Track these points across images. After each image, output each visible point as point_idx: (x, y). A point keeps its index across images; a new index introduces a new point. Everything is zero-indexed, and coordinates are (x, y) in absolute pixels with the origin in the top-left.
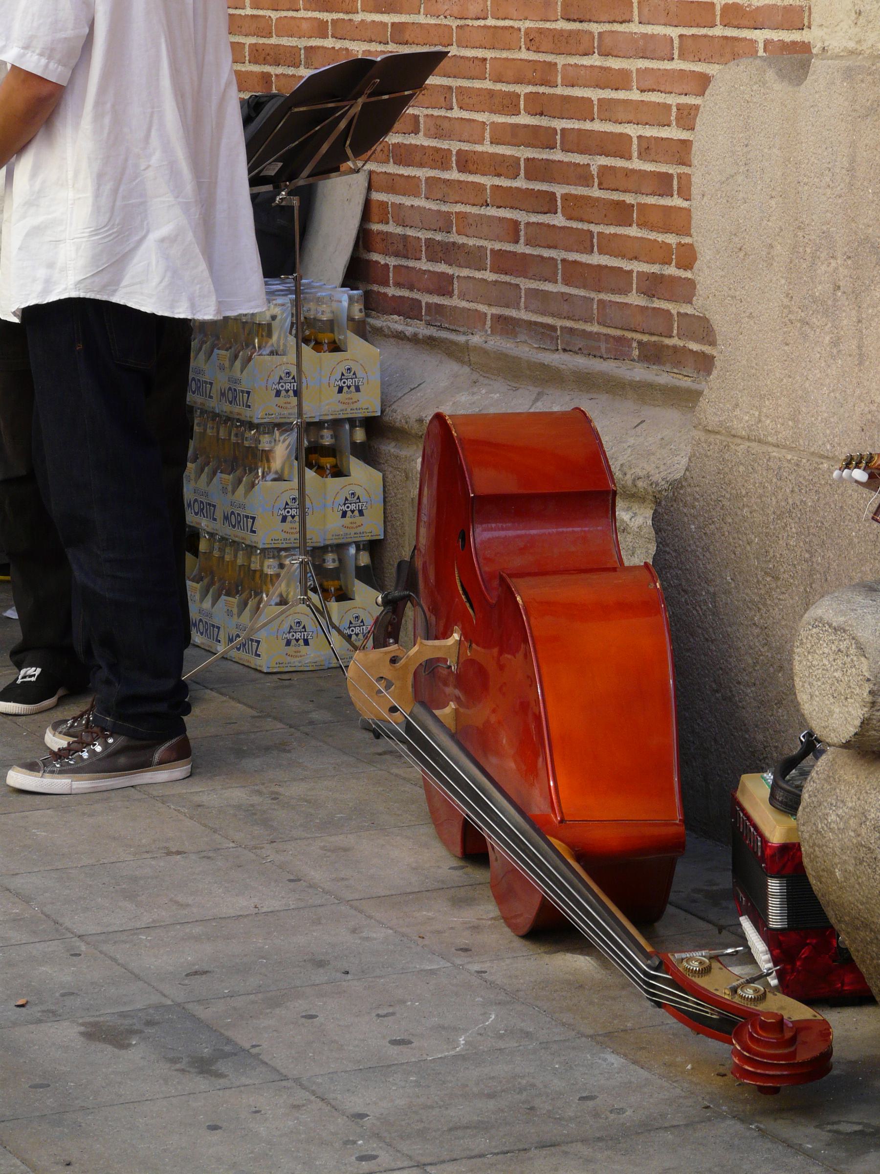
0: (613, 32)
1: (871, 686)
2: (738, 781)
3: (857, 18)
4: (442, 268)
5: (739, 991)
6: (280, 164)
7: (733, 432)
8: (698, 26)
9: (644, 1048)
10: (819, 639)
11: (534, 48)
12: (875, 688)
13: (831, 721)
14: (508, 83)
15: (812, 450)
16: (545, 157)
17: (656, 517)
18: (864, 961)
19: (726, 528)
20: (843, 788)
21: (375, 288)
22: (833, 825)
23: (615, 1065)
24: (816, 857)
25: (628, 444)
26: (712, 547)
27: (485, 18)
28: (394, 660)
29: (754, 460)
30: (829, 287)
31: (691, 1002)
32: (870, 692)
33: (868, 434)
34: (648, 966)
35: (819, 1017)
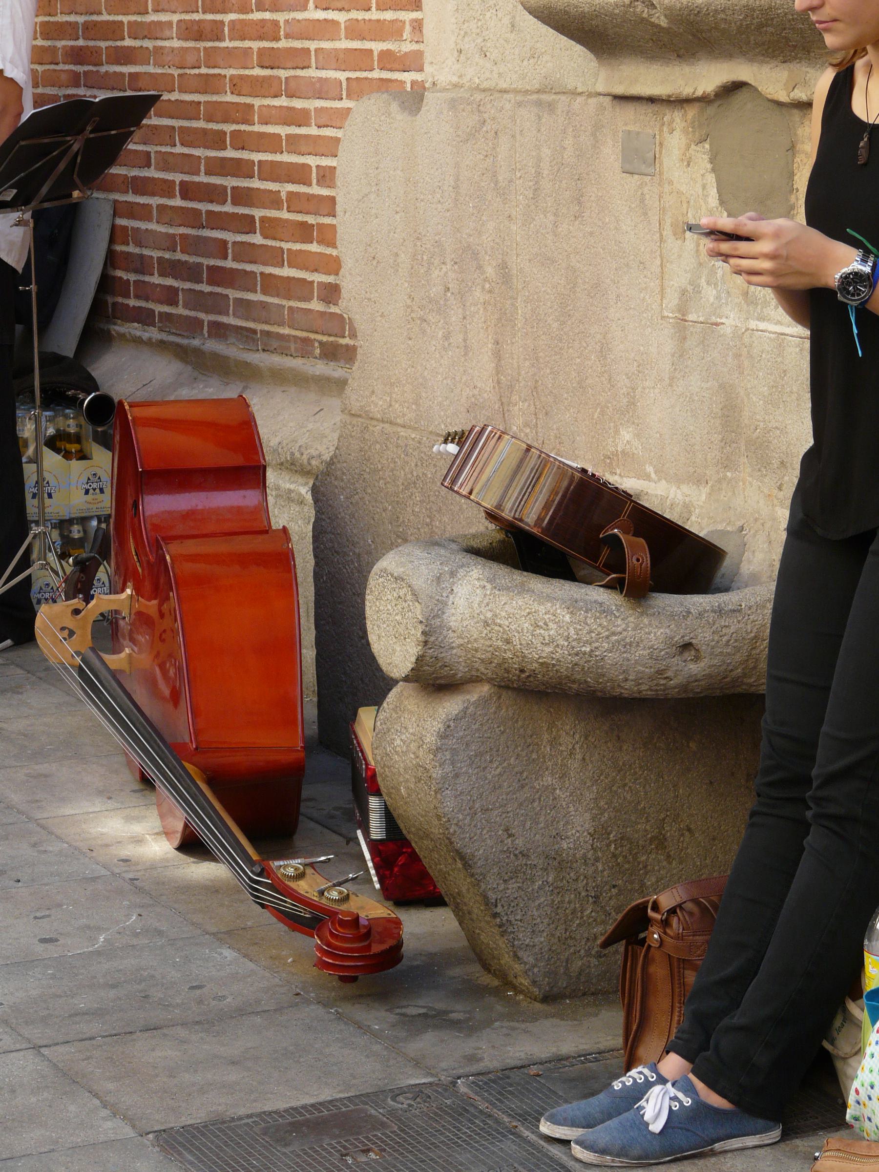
0: (296, 77)
1: (424, 627)
2: (355, 714)
3: (459, 56)
4: (170, 282)
5: (326, 893)
6: (15, 191)
7: (371, 415)
8: (360, 70)
9: (256, 944)
10: (384, 588)
11: (237, 92)
14: (217, 122)
16: (246, 185)
17: (315, 490)
18: (431, 867)
19: (367, 498)
21: (120, 300)
22: (398, 749)
27: (199, 67)
28: (77, 612)
29: (387, 439)
30: (440, 289)
31: (288, 904)
34: (252, 872)
35: (393, 916)
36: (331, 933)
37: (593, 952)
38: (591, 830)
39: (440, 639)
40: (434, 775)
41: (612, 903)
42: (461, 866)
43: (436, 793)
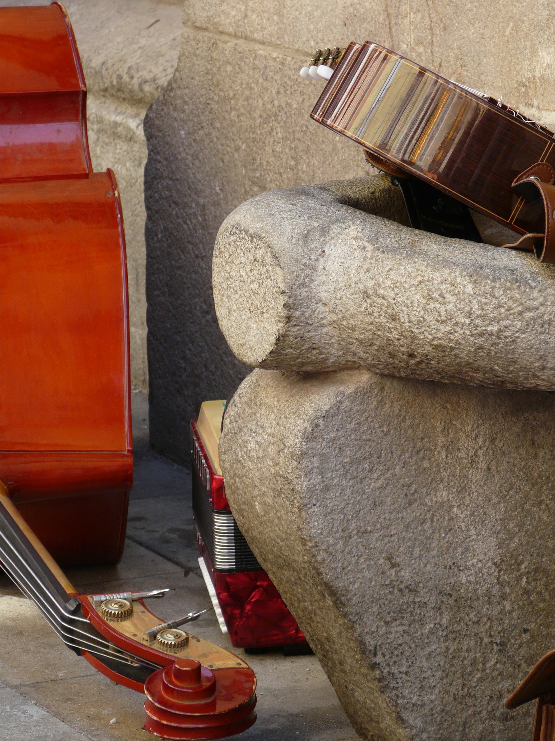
1: (286, 299)
2: (197, 410)
5: (159, 637)
7: (221, 28)
9: (70, 700)
12: (291, 301)
13: (248, 338)
15: (297, 46)
17: (148, 123)
18: (292, 604)
19: (215, 134)
20: (263, 413)
22: (252, 454)
23: (35, 718)
24: (237, 488)
25: (139, 45)
26: (201, 155)
29: (241, 59)
32: (284, 305)
33: (350, 28)
35: (244, 665)
36: (166, 687)
37: (498, 714)
38: (497, 560)
39: (307, 314)
40: (298, 488)
41: (522, 651)
42: (331, 603)
43: (300, 510)
